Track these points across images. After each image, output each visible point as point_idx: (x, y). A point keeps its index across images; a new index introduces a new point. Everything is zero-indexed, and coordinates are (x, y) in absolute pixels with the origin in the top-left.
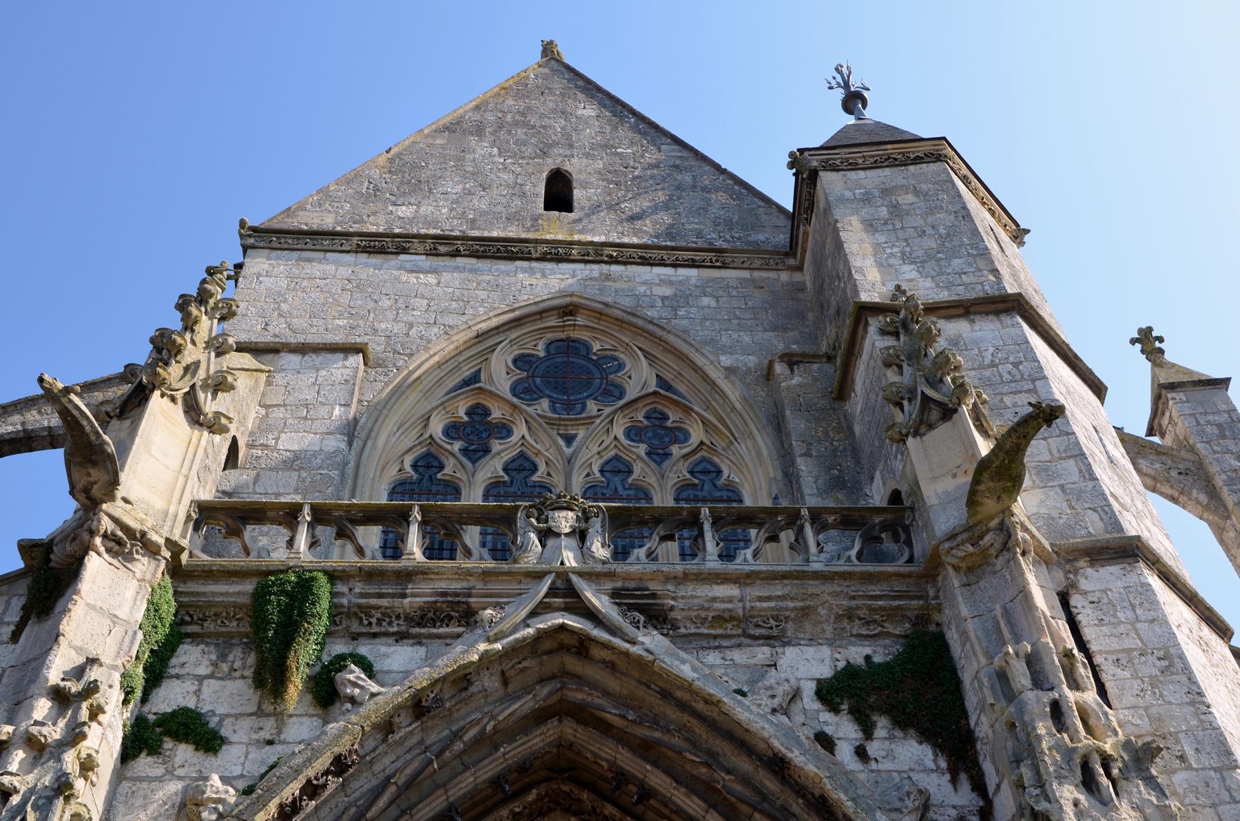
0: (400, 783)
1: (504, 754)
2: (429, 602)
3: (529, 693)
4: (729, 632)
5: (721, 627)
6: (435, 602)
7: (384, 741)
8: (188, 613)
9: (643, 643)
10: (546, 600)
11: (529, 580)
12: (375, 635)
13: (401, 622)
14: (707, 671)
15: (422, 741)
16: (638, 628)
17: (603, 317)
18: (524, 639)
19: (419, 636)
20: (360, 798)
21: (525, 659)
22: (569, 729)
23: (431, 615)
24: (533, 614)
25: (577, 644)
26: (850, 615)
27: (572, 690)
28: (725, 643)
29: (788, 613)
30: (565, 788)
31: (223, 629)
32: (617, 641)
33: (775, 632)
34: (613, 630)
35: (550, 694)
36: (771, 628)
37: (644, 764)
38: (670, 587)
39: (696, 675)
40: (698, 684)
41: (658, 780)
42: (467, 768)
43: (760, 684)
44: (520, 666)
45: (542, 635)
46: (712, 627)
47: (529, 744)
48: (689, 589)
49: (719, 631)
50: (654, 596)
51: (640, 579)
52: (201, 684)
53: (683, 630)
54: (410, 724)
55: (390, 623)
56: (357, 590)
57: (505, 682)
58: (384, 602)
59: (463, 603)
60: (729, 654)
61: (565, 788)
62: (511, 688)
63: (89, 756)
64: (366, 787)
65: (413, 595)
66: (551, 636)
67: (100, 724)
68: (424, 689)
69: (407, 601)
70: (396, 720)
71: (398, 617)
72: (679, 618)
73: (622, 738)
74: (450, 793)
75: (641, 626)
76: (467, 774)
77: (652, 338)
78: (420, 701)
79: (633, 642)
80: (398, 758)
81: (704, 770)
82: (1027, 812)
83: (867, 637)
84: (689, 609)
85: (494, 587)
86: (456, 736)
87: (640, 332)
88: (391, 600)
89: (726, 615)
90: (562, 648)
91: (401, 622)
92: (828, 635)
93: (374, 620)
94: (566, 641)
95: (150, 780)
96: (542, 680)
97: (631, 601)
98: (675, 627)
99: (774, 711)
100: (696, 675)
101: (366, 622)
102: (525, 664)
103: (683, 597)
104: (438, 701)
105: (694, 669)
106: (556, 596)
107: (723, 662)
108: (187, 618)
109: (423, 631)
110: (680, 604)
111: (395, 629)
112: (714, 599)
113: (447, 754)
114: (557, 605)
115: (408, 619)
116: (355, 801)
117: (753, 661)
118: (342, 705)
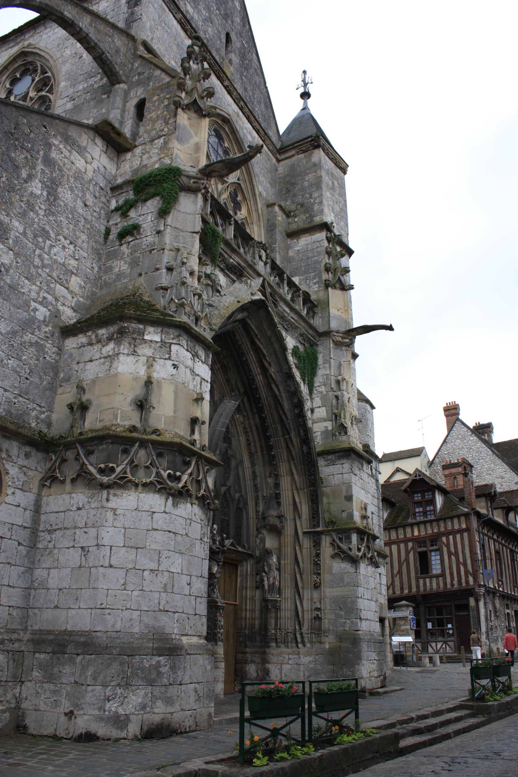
26: (301, 335)
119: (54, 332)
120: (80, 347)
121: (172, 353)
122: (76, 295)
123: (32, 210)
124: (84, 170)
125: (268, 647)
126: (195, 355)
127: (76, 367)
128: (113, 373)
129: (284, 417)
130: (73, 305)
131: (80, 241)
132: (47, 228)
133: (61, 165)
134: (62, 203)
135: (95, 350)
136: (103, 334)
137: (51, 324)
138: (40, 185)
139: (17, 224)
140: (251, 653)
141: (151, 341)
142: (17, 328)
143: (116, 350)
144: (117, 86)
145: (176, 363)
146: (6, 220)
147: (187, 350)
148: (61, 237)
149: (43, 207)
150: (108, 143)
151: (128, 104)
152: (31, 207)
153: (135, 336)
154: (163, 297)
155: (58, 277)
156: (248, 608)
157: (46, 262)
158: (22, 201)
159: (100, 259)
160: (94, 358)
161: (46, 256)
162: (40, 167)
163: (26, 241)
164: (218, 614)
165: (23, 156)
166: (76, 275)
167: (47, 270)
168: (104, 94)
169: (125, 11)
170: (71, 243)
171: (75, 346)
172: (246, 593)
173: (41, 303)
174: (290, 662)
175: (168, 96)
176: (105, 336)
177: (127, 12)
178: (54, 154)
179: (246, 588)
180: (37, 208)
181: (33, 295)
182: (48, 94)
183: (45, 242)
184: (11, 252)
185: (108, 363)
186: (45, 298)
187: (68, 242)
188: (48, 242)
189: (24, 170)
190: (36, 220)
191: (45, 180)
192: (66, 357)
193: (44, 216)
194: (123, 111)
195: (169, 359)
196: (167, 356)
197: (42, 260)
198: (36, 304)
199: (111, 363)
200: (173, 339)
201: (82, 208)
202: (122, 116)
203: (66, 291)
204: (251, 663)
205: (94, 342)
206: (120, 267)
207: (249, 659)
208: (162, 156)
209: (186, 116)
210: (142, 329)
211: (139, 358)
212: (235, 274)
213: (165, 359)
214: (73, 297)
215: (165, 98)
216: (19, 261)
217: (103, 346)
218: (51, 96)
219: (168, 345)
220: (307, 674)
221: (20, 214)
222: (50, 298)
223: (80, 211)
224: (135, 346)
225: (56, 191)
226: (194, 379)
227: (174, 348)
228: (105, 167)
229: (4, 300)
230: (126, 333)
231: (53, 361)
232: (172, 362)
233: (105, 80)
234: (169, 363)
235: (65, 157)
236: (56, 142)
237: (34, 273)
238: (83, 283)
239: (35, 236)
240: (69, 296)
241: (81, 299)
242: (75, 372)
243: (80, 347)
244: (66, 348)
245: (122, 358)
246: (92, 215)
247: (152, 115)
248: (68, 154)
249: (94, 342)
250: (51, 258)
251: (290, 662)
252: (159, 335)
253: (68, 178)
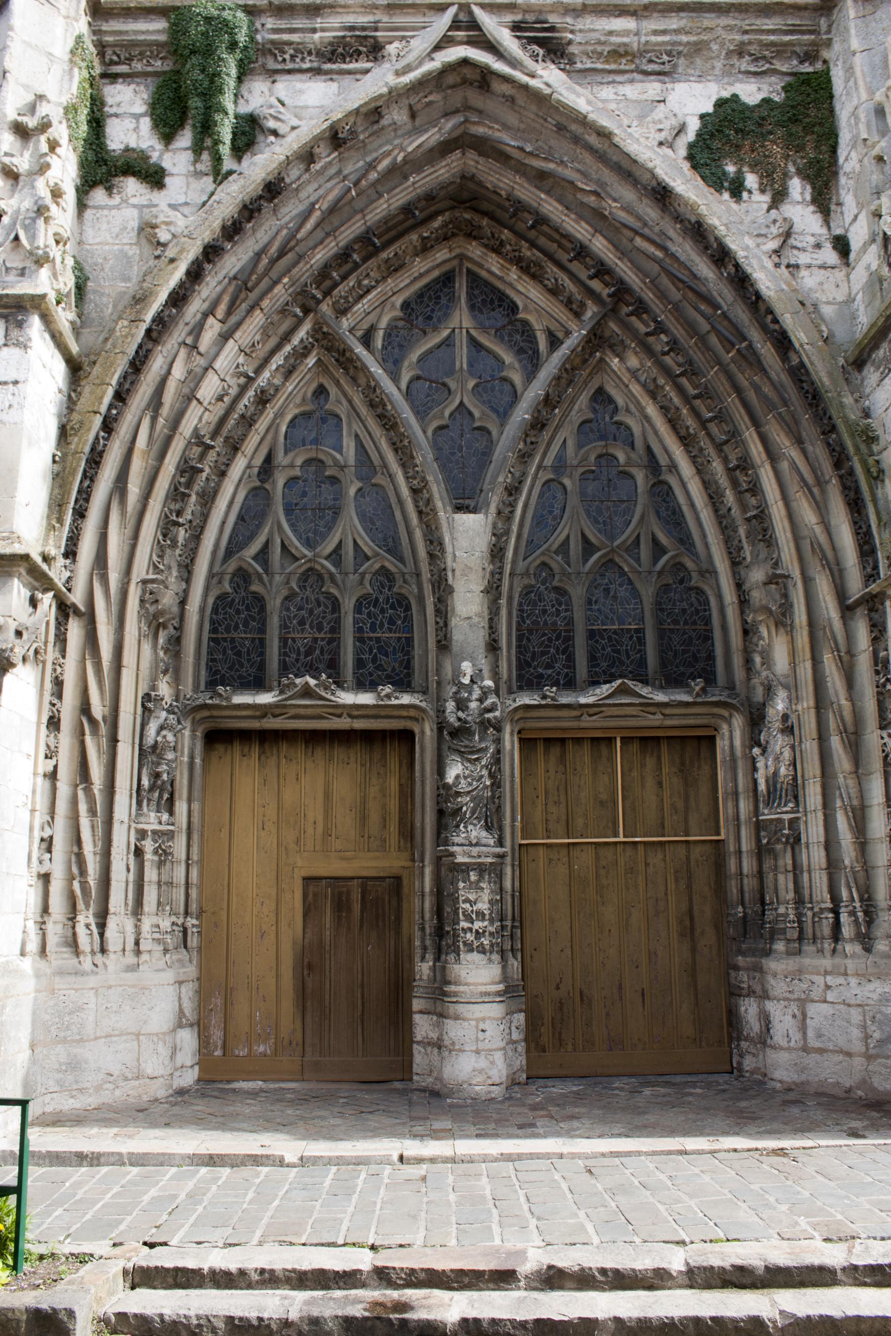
0: (325, 206)
1: (414, 183)
2: (337, 37)
3: (435, 126)
4: (622, 67)
5: (615, 62)
6: (344, 37)
7: (307, 170)
8: (115, 53)
9: (541, 77)
10: (449, 33)
11: (432, 13)
12: (289, 72)
13: (313, 58)
14: (601, 105)
15: (340, 172)
16: (537, 61)
18: (430, 73)
19: (327, 72)
20: (289, 222)
21: (430, 93)
22: (472, 162)
23: (340, 50)
24: (438, 47)
25: (479, 78)
26: (740, 51)
27: (474, 123)
28: (619, 78)
29: (681, 48)
30: (467, 216)
31: (150, 69)
32: (518, 75)
33: (667, 68)
34: (514, 63)
35: (455, 128)
36: (664, 63)
37: (538, 193)
38: (569, 20)
39: (590, 108)
40: (592, 116)
41: (551, 208)
42: (380, 196)
43: (649, 119)
44: (427, 100)
45: (449, 68)
46: (607, 62)
47: (436, 175)
48: (588, 22)
49: (613, 67)
50: (552, 29)
51: (540, 12)
52: (138, 122)
53: (579, 66)
54: (329, 155)
55: (303, 59)
56: (269, 26)
57: (413, 116)
58: (295, 37)
59: (371, 37)
60: (622, 89)
61: (467, 216)
62: (418, 121)
63: (56, 184)
64: (295, 212)
65: (323, 30)
66: (454, 70)
67: (59, 156)
68: (339, 120)
69: (317, 36)
70: (317, 150)
71: (310, 53)
72: (576, 52)
73: (521, 169)
74: (367, 218)
75: (540, 59)
76: (381, 201)
78: (336, 133)
79: (533, 76)
80: (320, 186)
81: (593, 198)
82: (880, 239)
84: (587, 43)
85: (400, 19)
86: (371, 166)
88: (301, 35)
89: (622, 50)
90: (465, 81)
91: (313, 58)
92: (717, 72)
93: (287, 57)
94: (468, 76)
95: (111, 208)
96: (447, 114)
97: (531, 34)
98: (572, 62)
99: (661, 144)
100: (590, 108)
101: (280, 59)
102: (430, 98)
103: (581, 31)
104: (353, 132)
105: (589, 103)
106: (458, 29)
107: (615, 97)
108: (115, 58)
109: (334, 66)
110: (578, 38)
111: (307, 65)
112: (611, 33)
113: (363, 182)
114: (459, 39)
115: (319, 54)
116: (287, 224)
117: (644, 97)
118: (266, 137)
125: (768, 953)
140: (747, 969)
156: (744, 847)
164: (461, 885)
172: (737, 806)
174: (830, 997)
179: (736, 794)
204: (748, 995)
207: (745, 986)
212: (356, 55)
220: (877, 1035)
251: (830, 997)
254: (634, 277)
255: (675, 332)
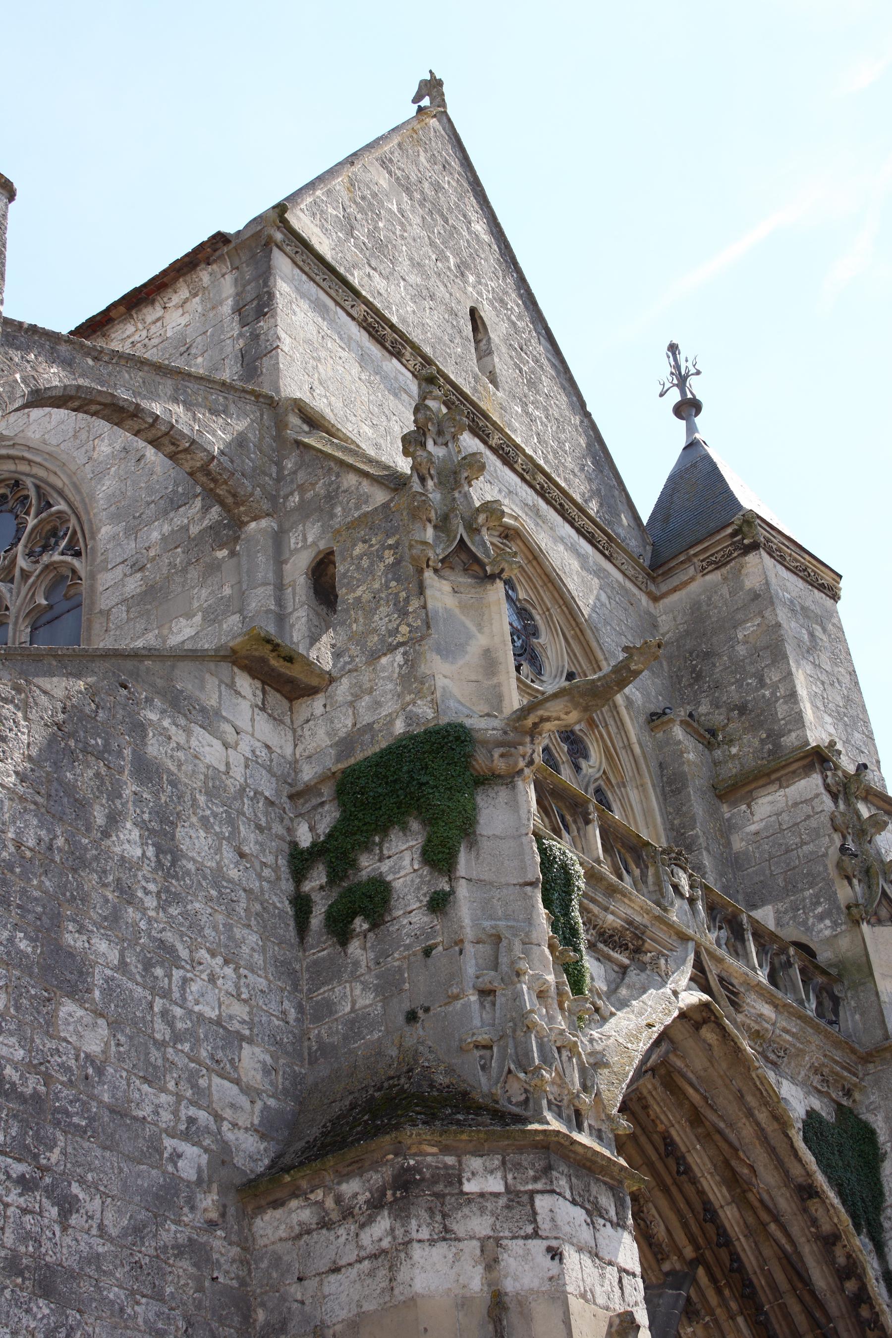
17: (534, 563)
37: (696, 1142)
77: (569, 617)
83: (819, 1091)
87: (561, 602)
109: (606, 949)
119: (225, 1206)
120: (299, 1236)
121: (539, 1218)
122: (259, 1093)
123: (129, 903)
124: (222, 768)
126: (594, 1211)
127: (296, 1291)
128: (402, 1298)
129: (818, 1315)
130: (256, 1122)
131: (245, 949)
132: (169, 936)
133: (173, 769)
134: (190, 866)
135: (342, 1240)
136: (355, 1195)
137: (215, 1187)
138: (136, 834)
139: (102, 946)
141: (482, 1195)
142: (143, 1215)
143: (399, 1232)
144: (253, 525)
145: (554, 1243)
146: (79, 944)
147: (574, 1202)
148: (203, 954)
149: (152, 887)
150: (264, 683)
151: (287, 567)
152: (127, 895)
153: (439, 1188)
154: (483, 1068)
155: (212, 1057)
157: (180, 1025)
158: (105, 885)
159: (296, 987)
160: (343, 1262)
161: (178, 1011)
162: (130, 788)
163: (130, 985)
165: (90, 773)
166: (250, 1041)
167: (186, 1047)
168: (221, 547)
169: (236, 333)
170: (226, 962)
171: (282, 1233)
173: (186, 1136)
175: (390, 542)
176: (362, 1199)
177: (241, 335)
178: (154, 748)
180: (140, 894)
181: (166, 1116)
182: (68, 559)
183: (169, 976)
184: (101, 1022)
185: (382, 1273)
186: (191, 1121)
187: (219, 960)
188: (177, 974)
189: (97, 807)
190: (143, 925)
191: (146, 817)
192: (264, 1265)
193: (156, 909)
194: (280, 587)
195: (536, 1235)
196: (529, 1229)
197: (171, 1024)
198: (175, 1142)
199: (390, 1269)
200: (535, 1179)
201: (237, 864)
202: (280, 601)
203: (235, 1089)
205: (335, 1216)
206: (354, 1003)
208: (408, 698)
209: (446, 586)
210: (452, 1167)
211: (461, 1245)
213: (526, 1237)
214: (252, 1102)
215: (384, 547)
216: (123, 1039)
217: (362, 1226)
218: (76, 562)
219: (525, 1199)
221: (105, 918)
222: (203, 1116)
223: (233, 873)
224: (445, 1216)
225: (173, 838)
226: (603, 1276)
227: (542, 1203)
228: (268, 747)
229: (105, 1148)
230: (417, 1183)
231: (235, 1283)
232: (545, 1243)
233: (215, 510)
234: (538, 1247)
235: (179, 747)
236: (153, 716)
237: (160, 1062)
238: (268, 1059)
239: (148, 966)
240: (244, 1101)
241: (272, 1102)
242: (295, 1305)
243: (299, 1236)
244: (261, 1242)
245: (417, 1252)
246: (260, 877)
247: (359, 593)
248: (179, 736)
249: (335, 1216)
250: (190, 1012)
252: (499, 1174)
253: (194, 800)
254: (752, 1258)
255: (777, 1326)
